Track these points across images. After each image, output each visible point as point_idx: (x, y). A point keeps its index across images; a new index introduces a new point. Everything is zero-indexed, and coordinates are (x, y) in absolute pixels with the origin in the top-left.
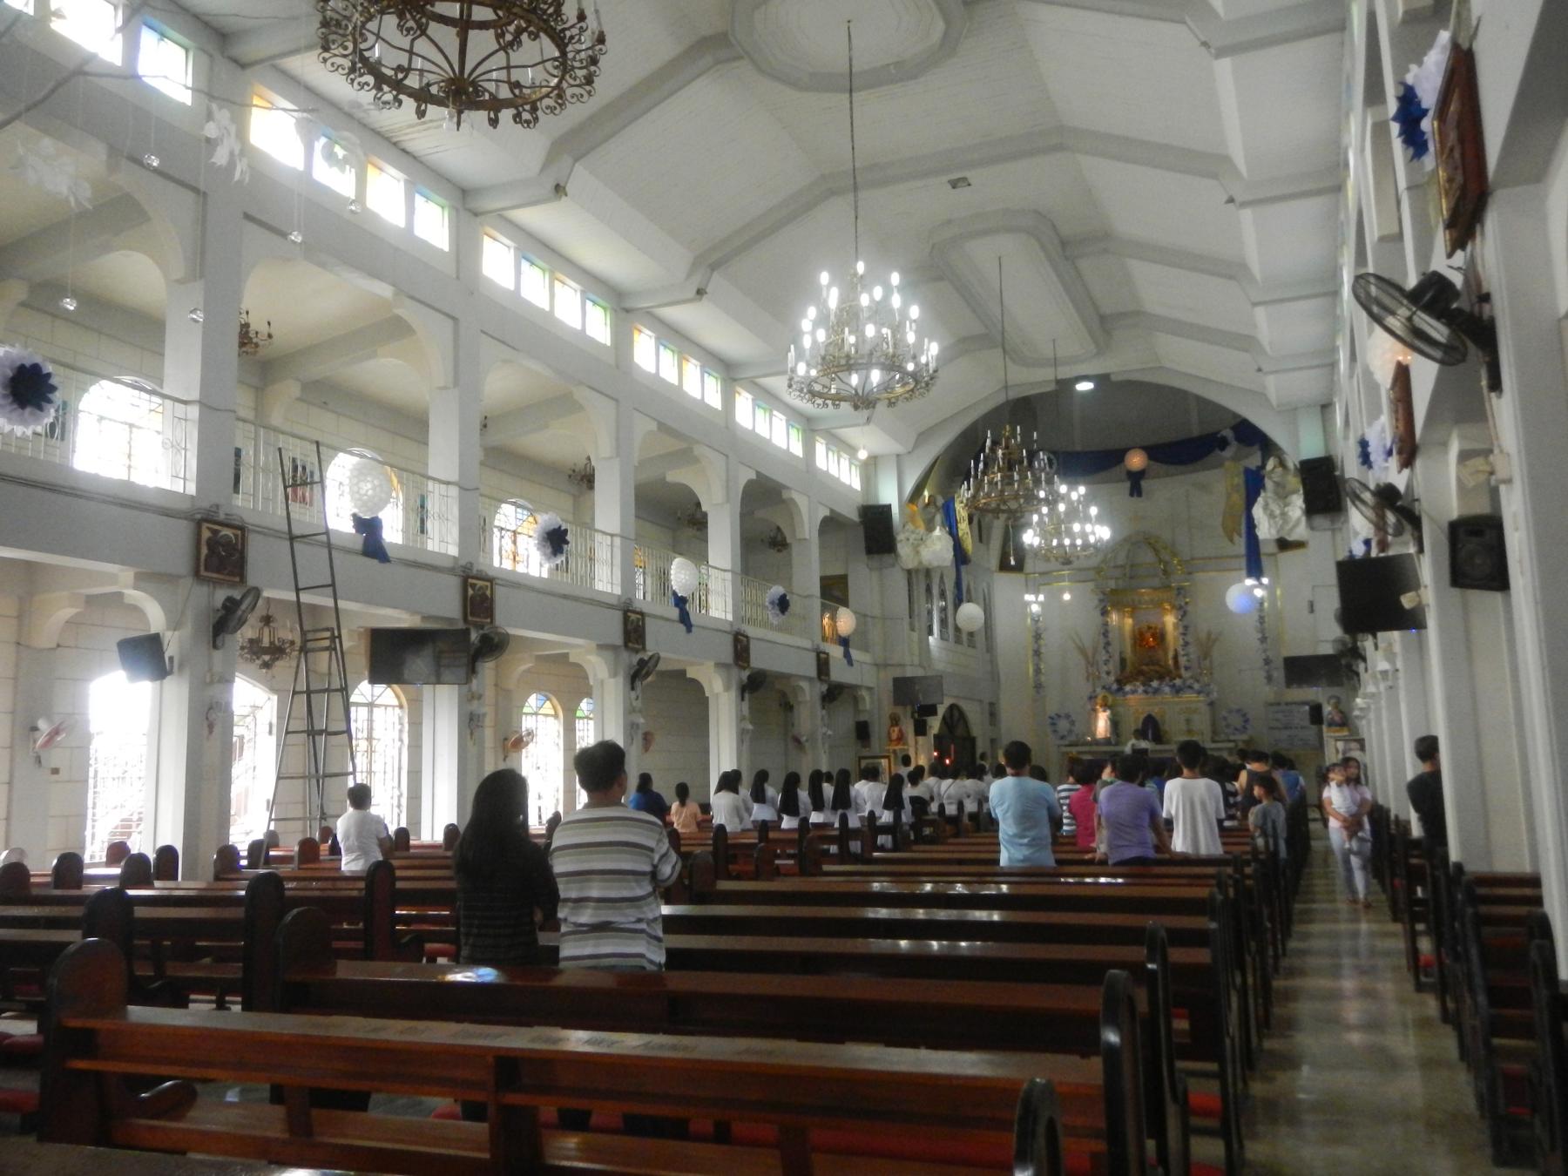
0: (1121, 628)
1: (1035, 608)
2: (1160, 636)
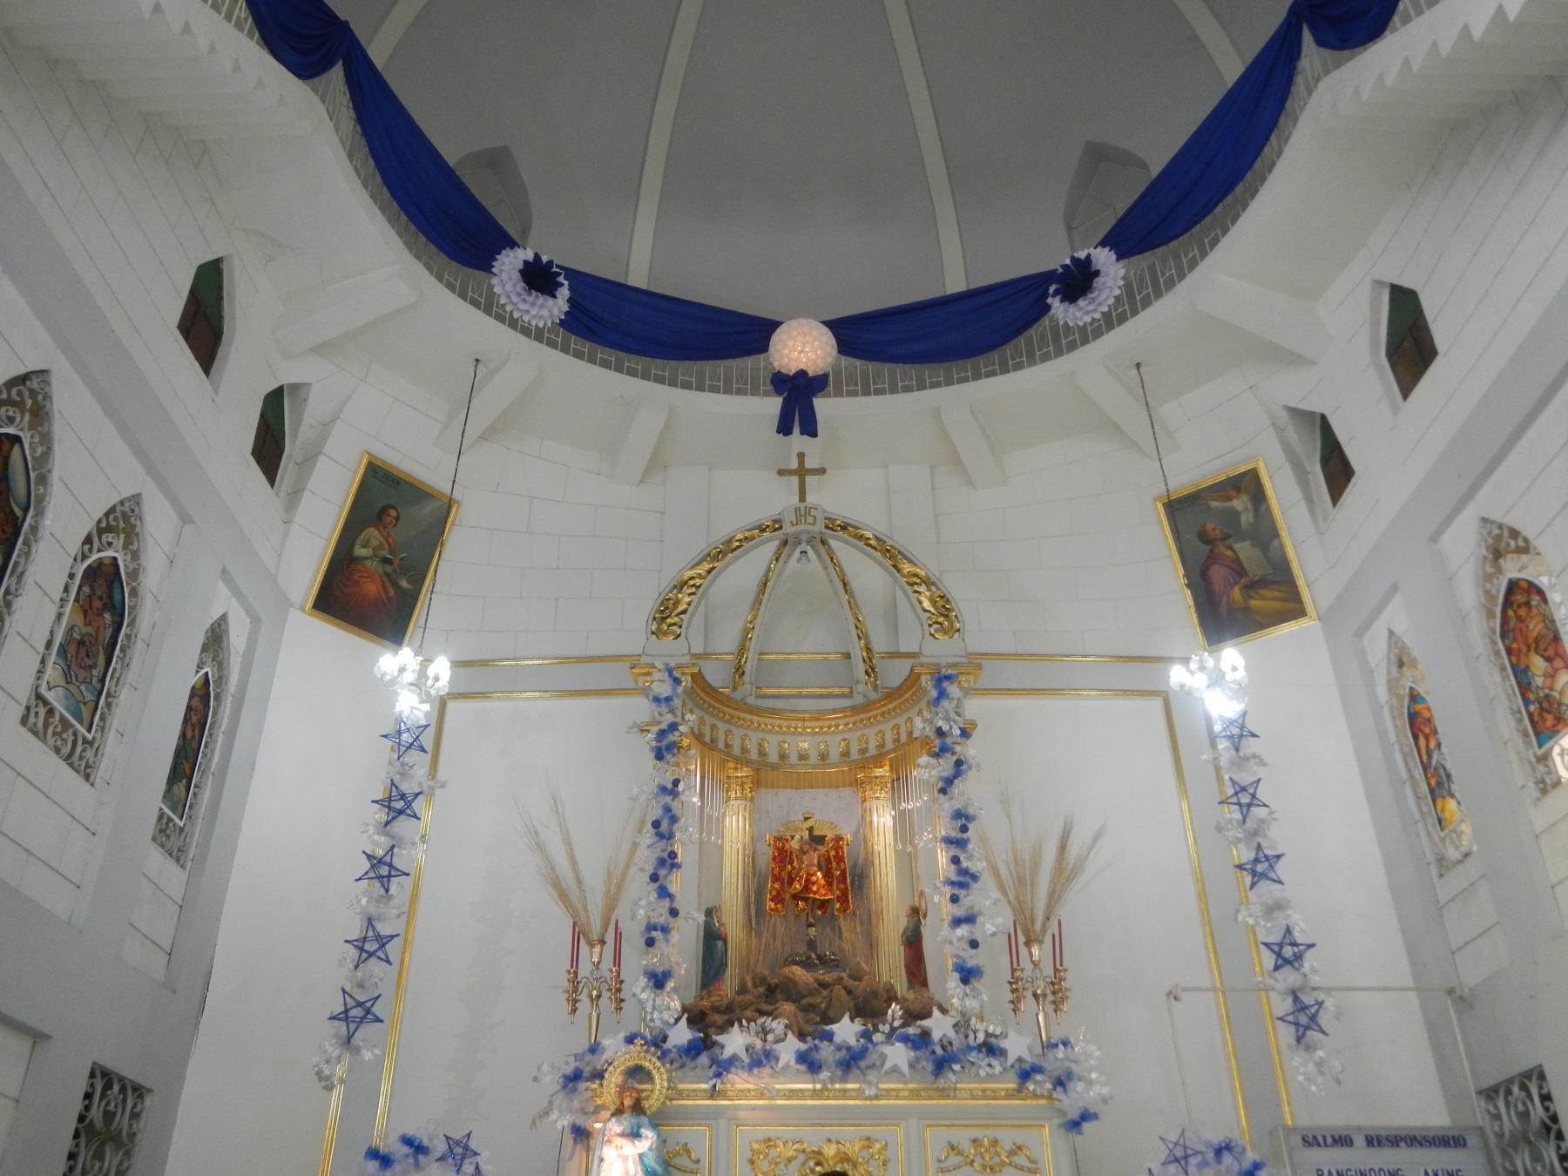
0: (710, 825)
1: (411, 706)
2: (846, 875)
